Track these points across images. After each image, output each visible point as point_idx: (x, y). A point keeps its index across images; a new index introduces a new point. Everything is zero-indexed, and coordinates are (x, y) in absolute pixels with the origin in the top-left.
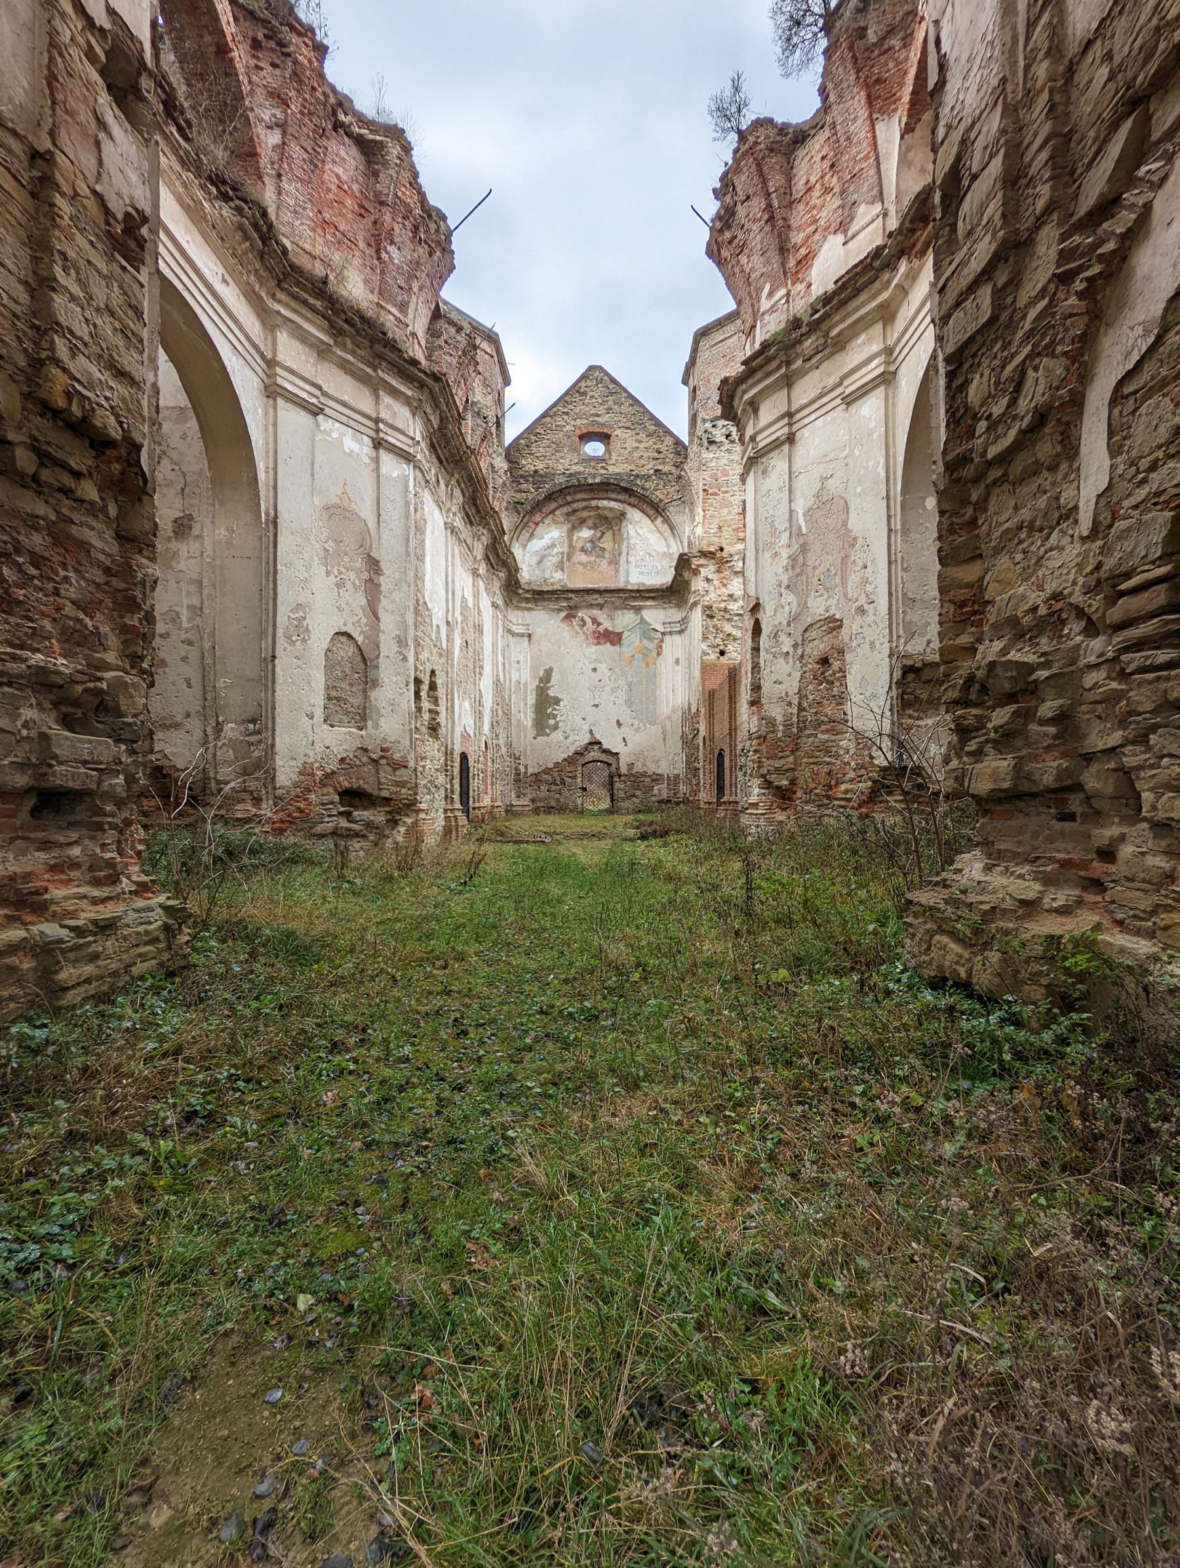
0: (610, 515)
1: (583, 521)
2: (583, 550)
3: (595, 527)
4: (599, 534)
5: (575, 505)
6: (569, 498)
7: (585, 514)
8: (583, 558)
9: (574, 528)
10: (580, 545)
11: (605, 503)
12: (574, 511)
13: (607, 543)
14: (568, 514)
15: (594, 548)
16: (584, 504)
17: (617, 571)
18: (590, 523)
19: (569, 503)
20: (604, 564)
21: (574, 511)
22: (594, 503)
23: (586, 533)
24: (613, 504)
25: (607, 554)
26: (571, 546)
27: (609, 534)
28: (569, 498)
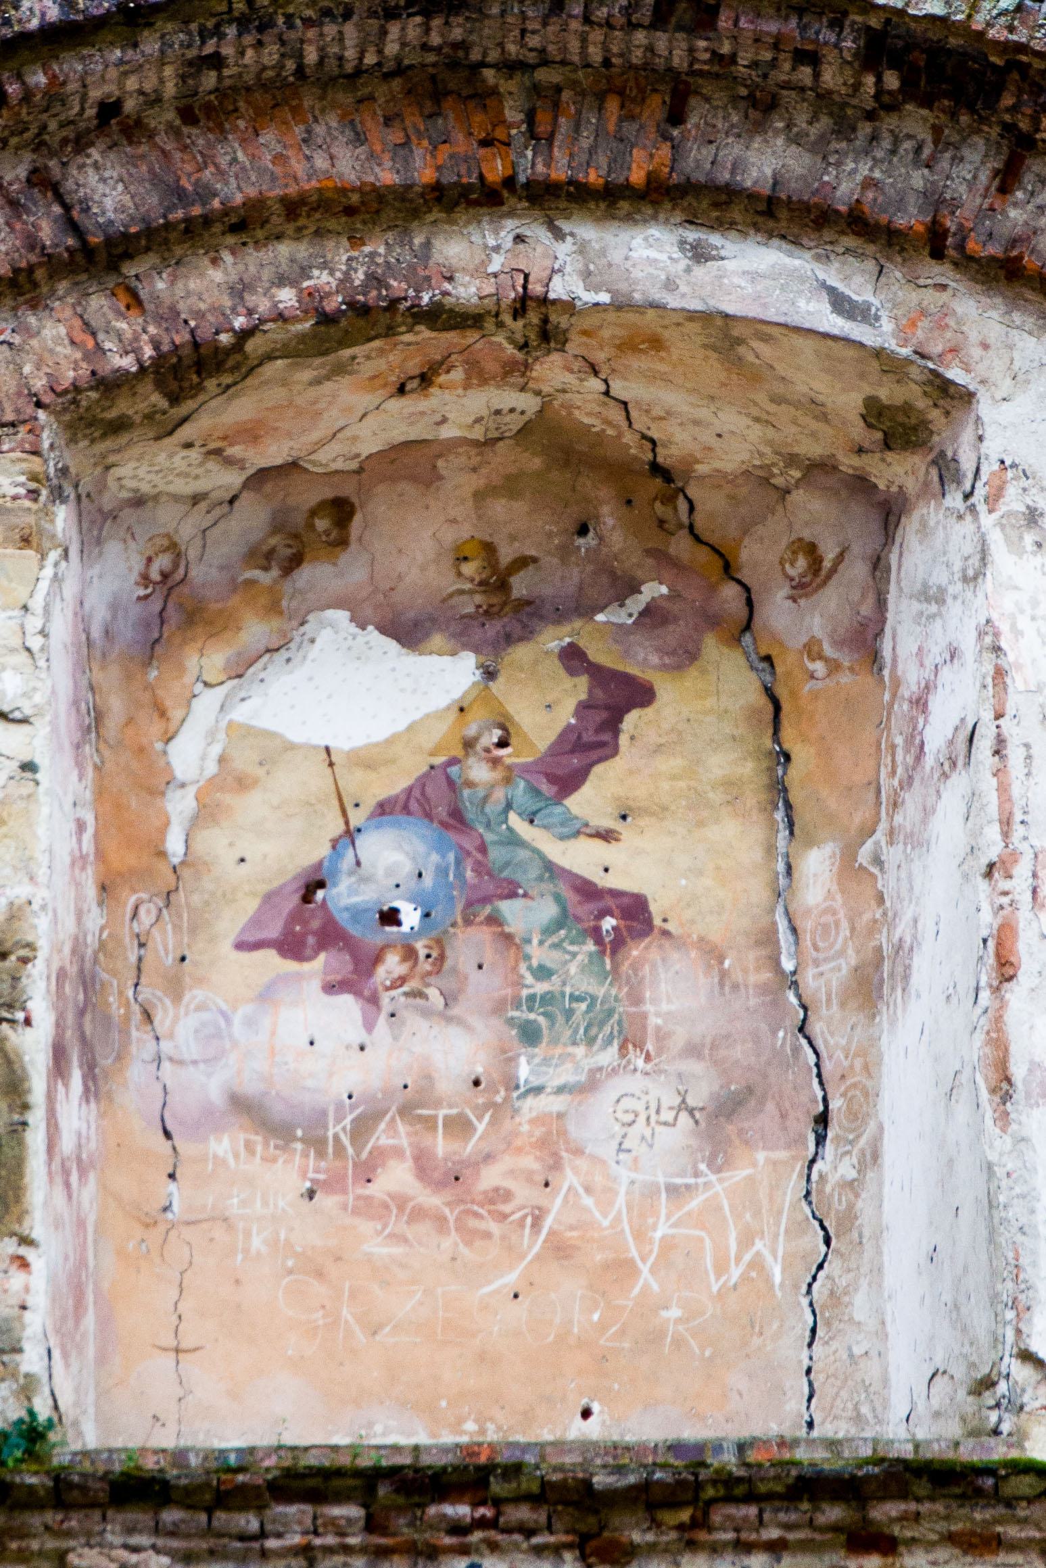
0: (712, 431)
1: (310, 527)
2: (306, 922)
3: (495, 607)
4: (545, 708)
5: (205, 290)
6: (110, 191)
7: (346, 417)
8: (313, 1037)
9: (170, 617)
10: (260, 849)
11: (647, 257)
12: (194, 368)
13: (671, 820)
14: (95, 411)
15: (484, 890)
16: (336, 269)
17: (831, 1229)
18: (414, 545)
19: (100, 258)
20: (625, 1133)
21: (194, 368)
22: (475, 259)
23: (353, 696)
24: (757, 276)
25: (673, 991)
26: (131, 862)
27: (694, 722)
28: (110, 191)
